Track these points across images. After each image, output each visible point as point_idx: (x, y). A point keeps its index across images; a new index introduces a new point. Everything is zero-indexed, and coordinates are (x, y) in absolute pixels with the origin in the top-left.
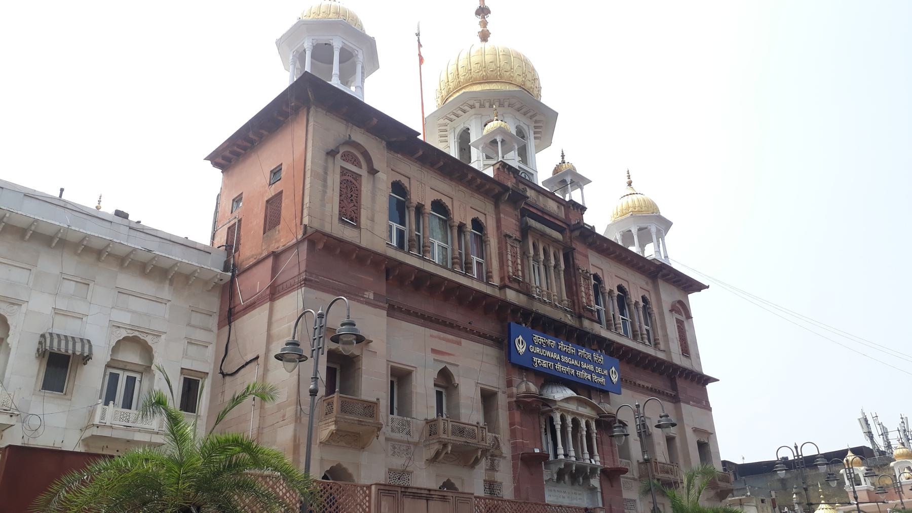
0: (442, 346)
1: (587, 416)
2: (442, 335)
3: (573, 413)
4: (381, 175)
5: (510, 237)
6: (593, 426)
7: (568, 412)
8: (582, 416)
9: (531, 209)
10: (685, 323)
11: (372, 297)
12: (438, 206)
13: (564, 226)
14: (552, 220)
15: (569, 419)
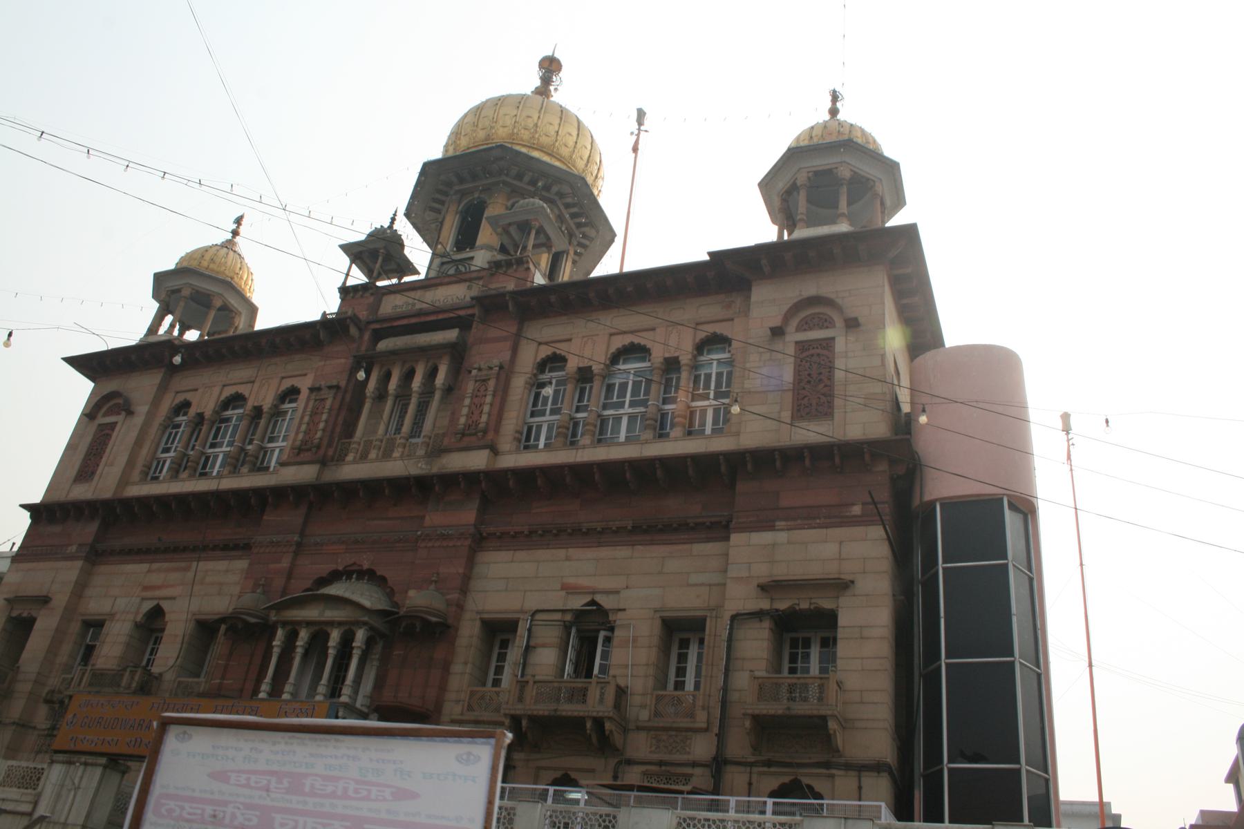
0: (156, 579)
1: (340, 624)
2: (166, 565)
3: (309, 624)
4: (142, 410)
5: (319, 389)
6: (360, 635)
7: (299, 623)
8: (332, 624)
9: (395, 324)
10: (840, 345)
11: (74, 548)
12: (236, 400)
13: (470, 312)
14: (441, 317)
15: (304, 635)
